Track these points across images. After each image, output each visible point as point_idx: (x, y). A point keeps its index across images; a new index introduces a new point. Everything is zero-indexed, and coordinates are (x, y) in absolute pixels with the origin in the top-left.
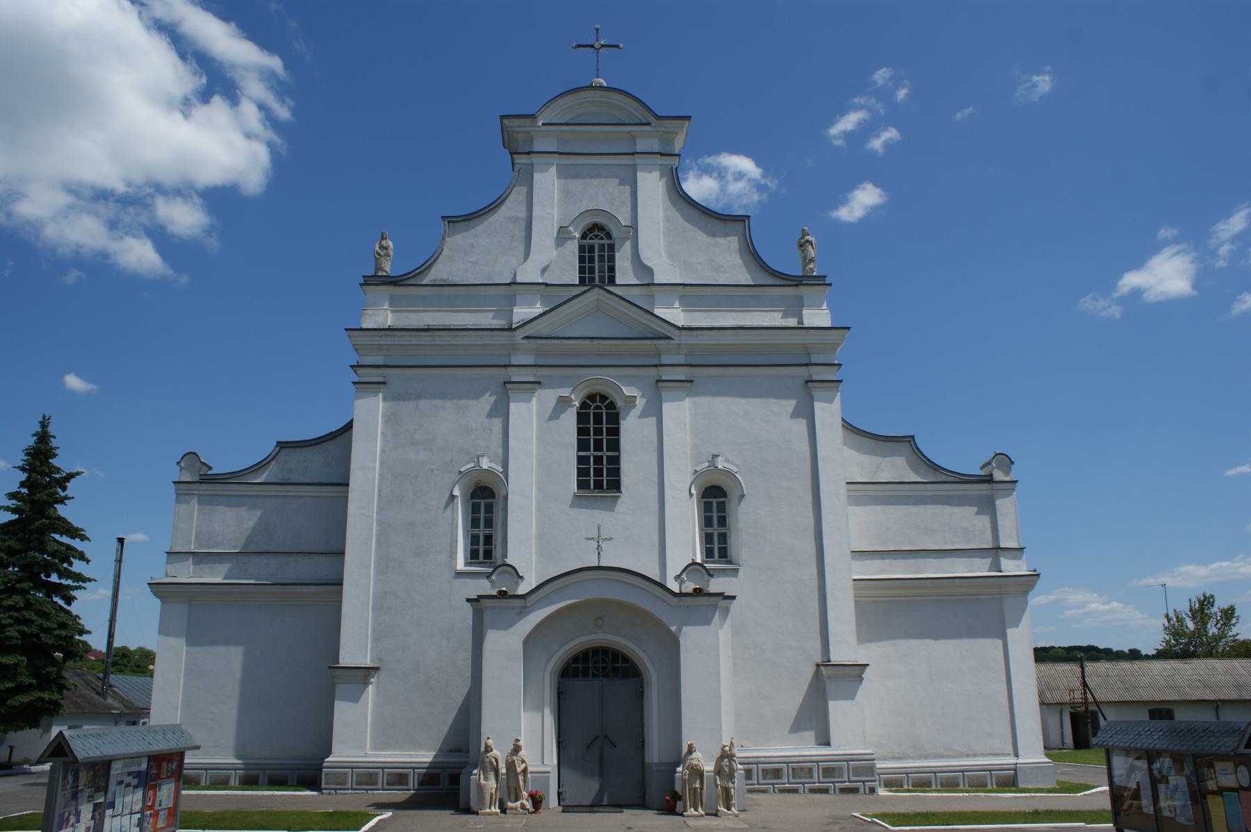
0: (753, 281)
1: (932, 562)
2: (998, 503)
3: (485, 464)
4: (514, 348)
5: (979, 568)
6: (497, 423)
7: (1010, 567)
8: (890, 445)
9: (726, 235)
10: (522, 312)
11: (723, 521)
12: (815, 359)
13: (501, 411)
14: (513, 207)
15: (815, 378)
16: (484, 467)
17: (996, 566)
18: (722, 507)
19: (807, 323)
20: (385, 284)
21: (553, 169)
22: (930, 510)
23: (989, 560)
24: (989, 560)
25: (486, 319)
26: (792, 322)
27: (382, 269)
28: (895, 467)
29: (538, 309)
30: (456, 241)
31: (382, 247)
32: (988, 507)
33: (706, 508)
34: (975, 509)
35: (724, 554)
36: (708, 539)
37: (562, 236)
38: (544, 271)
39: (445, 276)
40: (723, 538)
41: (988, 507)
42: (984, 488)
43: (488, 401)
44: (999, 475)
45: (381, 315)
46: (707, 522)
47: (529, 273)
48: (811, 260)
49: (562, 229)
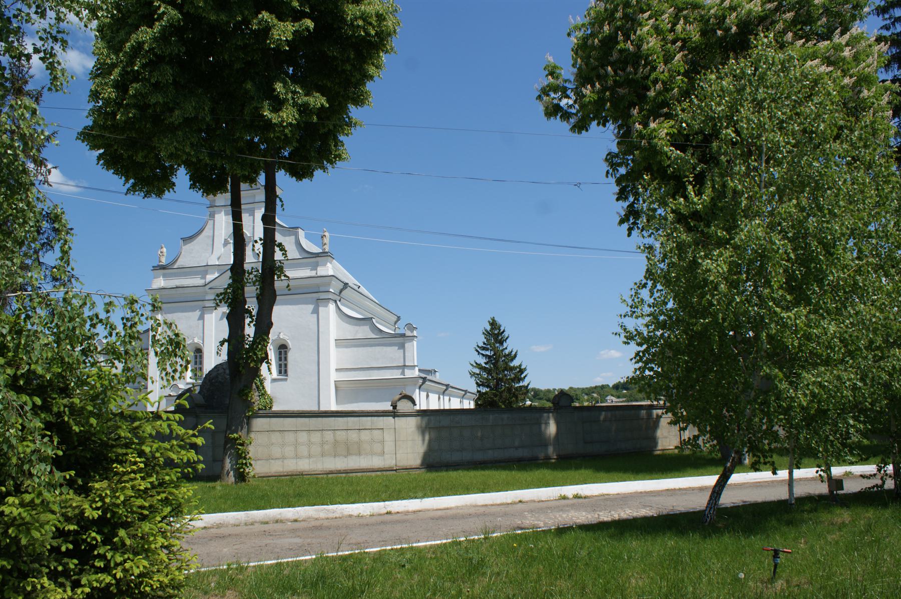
0: (300, 255)
1: (376, 372)
2: (406, 345)
3: (196, 341)
4: (206, 293)
5: (396, 374)
6: (201, 322)
7: (409, 374)
8: (362, 322)
9: (290, 236)
10: (210, 277)
11: (286, 359)
12: (322, 289)
13: (201, 318)
14: (207, 232)
15: (321, 298)
16: (196, 341)
17: (403, 373)
18: (286, 353)
19: (319, 274)
20: (160, 269)
21: (223, 213)
22: (378, 349)
23: (401, 370)
24: (401, 370)
25: (198, 281)
26: (313, 273)
27: (160, 261)
28: (364, 332)
29: (216, 275)
30: (186, 248)
31: (161, 252)
32: (402, 346)
33: (280, 353)
34: (397, 348)
35: (286, 371)
36: (280, 366)
37: (226, 243)
38: (218, 259)
39: (182, 264)
40: (286, 365)
41: (402, 346)
42: (400, 340)
43: (198, 313)
44: (408, 333)
45: (160, 282)
46: (280, 359)
47: (213, 261)
48: (325, 244)
49: (226, 240)
